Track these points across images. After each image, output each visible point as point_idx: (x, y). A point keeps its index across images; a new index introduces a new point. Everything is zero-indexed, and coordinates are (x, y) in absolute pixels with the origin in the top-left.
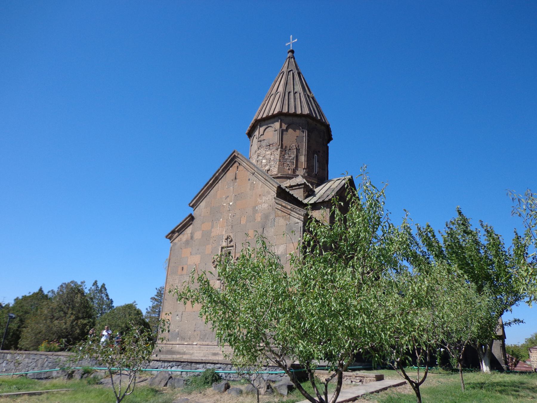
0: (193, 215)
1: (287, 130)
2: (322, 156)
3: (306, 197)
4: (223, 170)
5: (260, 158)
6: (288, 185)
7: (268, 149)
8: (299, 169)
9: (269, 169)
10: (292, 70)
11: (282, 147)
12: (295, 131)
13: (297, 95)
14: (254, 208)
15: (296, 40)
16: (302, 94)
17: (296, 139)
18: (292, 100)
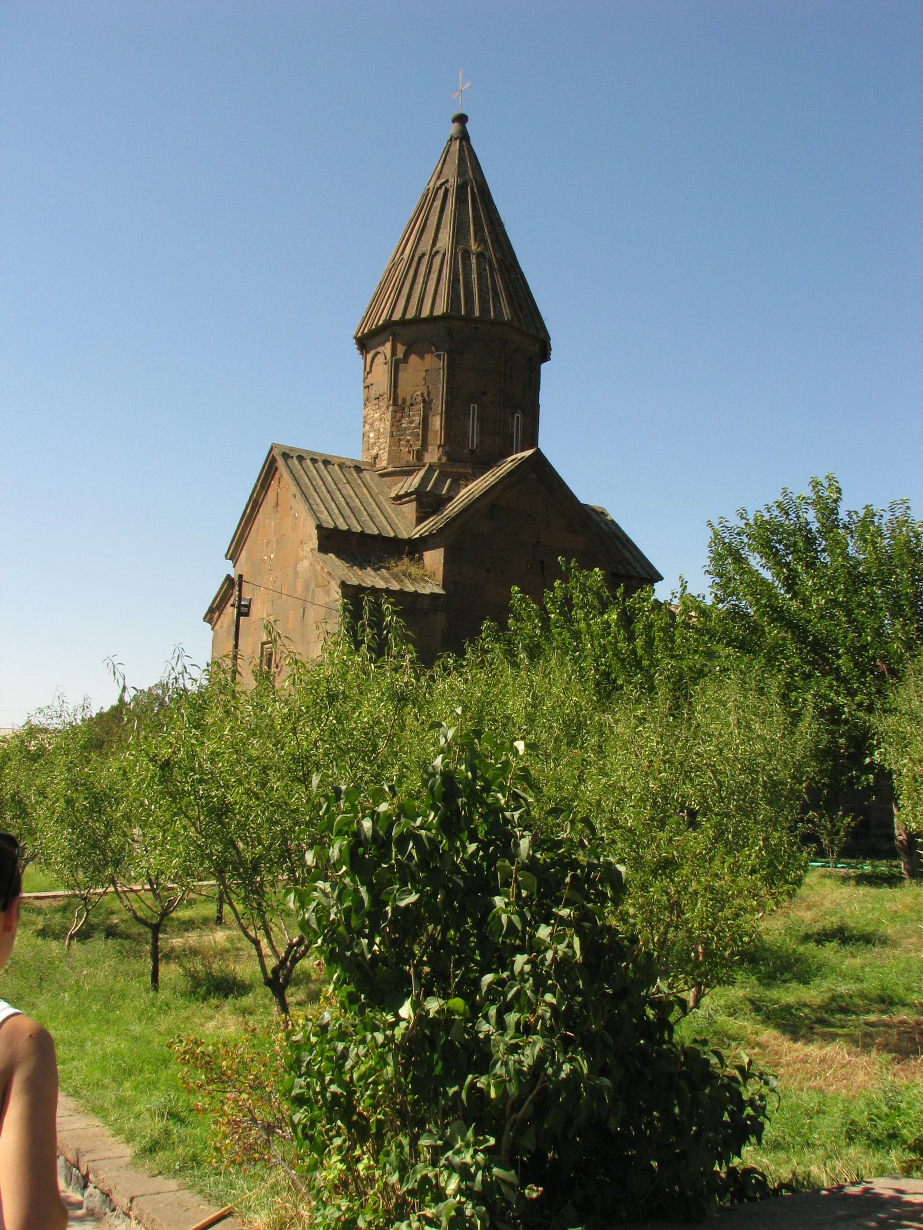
0: (233, 576)
1: (406, 359)
2: (492, 402)
3: (420, 520)
4: (262, 486)
5: (367, 427)
6: (393, 495)
8: (430, 448)
10: (447, 181)
11: (395, 404)
12: (422, 358)
13: (438, 260)
14: (296, 567)
15: (468, 85)
16: (448, 256)
17: (424, 379)
18: (420, 280)
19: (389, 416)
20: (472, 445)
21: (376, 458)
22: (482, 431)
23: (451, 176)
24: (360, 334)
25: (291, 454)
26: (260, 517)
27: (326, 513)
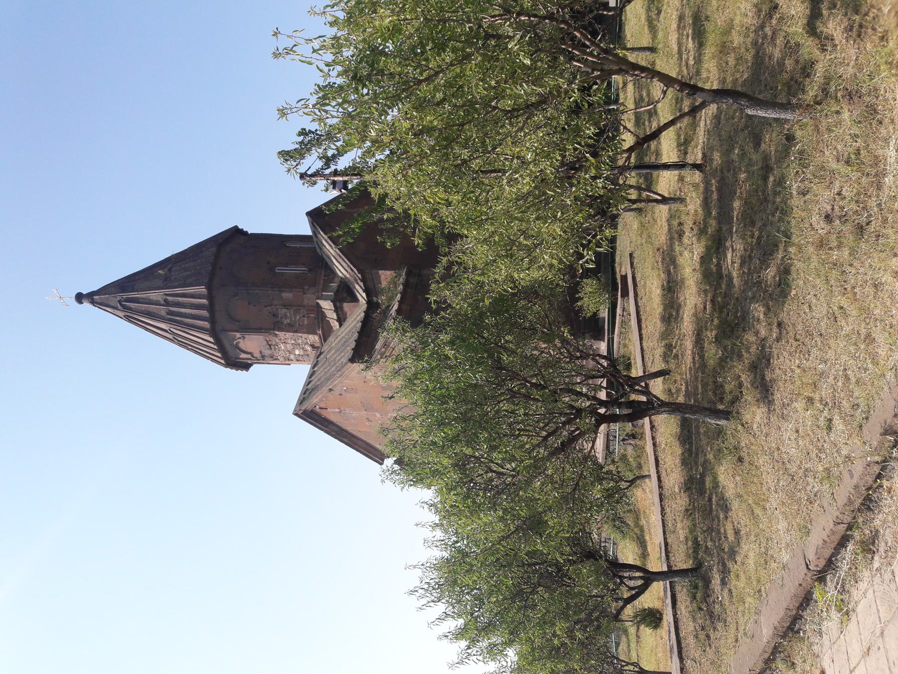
3: (355, 299)
5: (292, 357)
6: (337, 324)
7: (277, 348)
9: (311, 345)
10: (120, 302)
13: (170, 298)
16: (168, 291)
17: (255, 306)
18: (183, 310)
19: (281, 334)
20: (306, 270)
21: (313, 346)
22: (296, 264)
23: (114, 300)
24: (223, 361)
25: (302, 399)
26: (349, 429)
27: (342, 360)
